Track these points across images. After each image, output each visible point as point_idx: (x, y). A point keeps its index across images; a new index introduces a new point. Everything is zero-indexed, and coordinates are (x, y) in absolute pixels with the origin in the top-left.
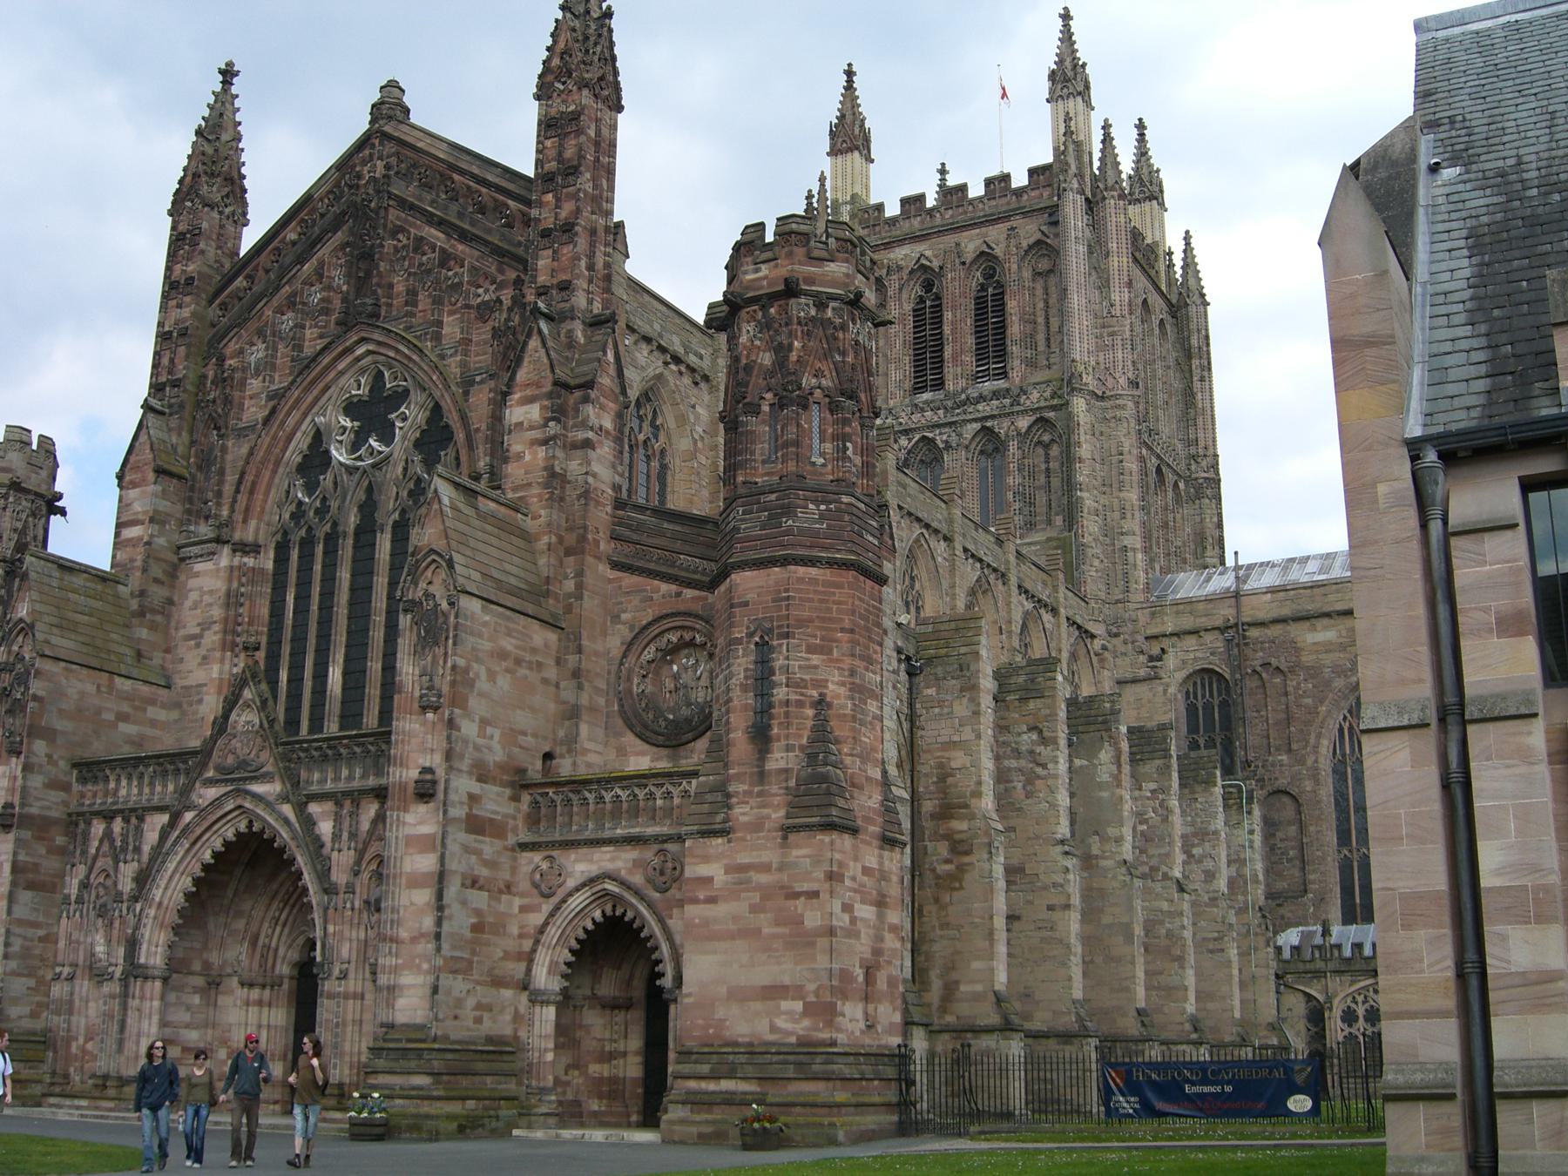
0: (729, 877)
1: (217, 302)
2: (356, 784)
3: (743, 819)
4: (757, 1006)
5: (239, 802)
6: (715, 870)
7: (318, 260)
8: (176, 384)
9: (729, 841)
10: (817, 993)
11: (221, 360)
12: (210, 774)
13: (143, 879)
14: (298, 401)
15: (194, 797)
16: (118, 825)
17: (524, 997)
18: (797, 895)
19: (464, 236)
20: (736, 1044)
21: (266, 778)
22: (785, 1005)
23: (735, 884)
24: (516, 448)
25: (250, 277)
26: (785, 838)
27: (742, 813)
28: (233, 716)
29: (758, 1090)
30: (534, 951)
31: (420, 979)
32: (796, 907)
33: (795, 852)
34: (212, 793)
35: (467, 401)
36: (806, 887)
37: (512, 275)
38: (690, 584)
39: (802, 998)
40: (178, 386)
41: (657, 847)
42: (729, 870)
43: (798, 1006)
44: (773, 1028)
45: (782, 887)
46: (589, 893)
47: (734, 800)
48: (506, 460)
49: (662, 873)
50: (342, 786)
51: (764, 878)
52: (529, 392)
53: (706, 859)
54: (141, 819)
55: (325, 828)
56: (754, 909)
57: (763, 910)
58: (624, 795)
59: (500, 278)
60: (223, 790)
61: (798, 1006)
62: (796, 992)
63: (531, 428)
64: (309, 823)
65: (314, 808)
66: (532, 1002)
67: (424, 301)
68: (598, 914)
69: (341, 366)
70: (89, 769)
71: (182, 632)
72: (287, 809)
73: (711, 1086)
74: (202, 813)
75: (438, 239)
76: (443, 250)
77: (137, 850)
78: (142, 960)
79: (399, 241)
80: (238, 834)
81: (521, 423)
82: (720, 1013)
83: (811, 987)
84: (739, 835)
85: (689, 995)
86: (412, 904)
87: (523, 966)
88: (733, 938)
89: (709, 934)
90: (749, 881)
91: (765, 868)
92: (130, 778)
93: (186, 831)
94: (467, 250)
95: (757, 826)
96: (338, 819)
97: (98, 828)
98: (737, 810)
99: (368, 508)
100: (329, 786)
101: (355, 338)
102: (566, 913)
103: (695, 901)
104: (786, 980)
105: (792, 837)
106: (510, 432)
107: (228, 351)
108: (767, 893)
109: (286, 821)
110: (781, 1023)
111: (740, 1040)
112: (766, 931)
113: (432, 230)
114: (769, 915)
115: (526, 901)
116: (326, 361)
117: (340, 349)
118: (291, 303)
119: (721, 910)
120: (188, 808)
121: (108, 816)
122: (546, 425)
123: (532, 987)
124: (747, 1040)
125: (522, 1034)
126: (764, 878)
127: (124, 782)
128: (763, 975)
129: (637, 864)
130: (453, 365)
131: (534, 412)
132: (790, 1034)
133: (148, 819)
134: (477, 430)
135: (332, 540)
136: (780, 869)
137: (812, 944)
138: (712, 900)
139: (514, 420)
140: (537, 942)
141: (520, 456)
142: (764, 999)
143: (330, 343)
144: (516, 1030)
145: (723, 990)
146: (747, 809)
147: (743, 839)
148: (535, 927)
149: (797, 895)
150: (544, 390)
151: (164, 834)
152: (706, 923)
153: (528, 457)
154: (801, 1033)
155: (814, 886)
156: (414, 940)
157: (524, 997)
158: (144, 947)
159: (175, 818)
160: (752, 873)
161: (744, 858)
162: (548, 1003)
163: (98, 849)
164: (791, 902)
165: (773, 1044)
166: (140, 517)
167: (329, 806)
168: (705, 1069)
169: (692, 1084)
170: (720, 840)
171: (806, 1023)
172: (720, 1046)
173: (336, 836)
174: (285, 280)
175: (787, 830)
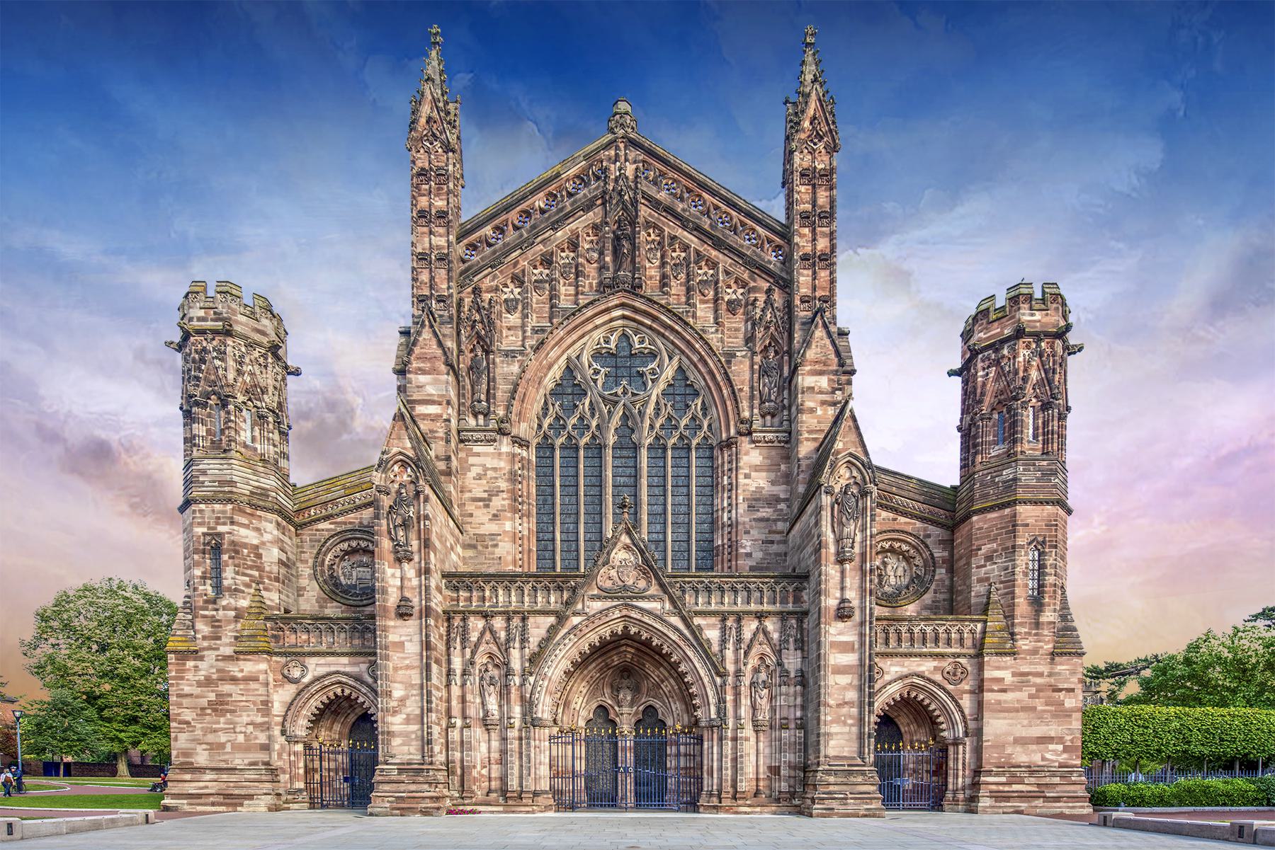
0: (1015, 679)
1: (466, 241)
2: (740, 607)
3: (1024, 647)
5: (625, 612)
6: (1007, 676)
7: (572, 231)
8: (441, 300)
9: (1015, 659)
10: (1072, 741)
11: (477, 291)
12: (596, 592)
13: (535, 660)
14: (562, 339)
15: (580, 606)
16: (498, 623)
18: (1060, 690)
19: (719, 244)
21: (651, 598)
24: (809, 404)
25: (500, 230)
27: (1024, 644)
28: (613, 555)
33: (1059, 667)
34: (598, 605)
35: (730, 368)
36: (1066, 686)
37: (765, 285)
38: (904, 514)
40: (444, 301)
42: (1014, 674)
47: (1018, 637)
48: (799, 411)
50: (726, 608)
51: (1038, 680)
52: (818, 367)
53: (998, 668)
54: (524, 619)
55: (712, 634)
56: (1031, 696)
57: (1038, 698)
58: (929, 630)
59: (752, 284)
60: (609, 604)
61: (1060, 747)
62: (1060, 740)
63: (821, 392)
64: (696, 632)
65: (697, 621)
67: (676, 288)
69: (598, 321)
70: (455, 580)
71: (467, 495)
72: (675, 621)
74: (590, 618)
75: (691, 241)
76: (698, 253)
77: (524, 641)
78: (539, 715)
79: (649, 235)
80: (613, 634)
81: (813, 388)
83: (1069, 738)
88: (1017, 711)
89: (1002, 709)
90: (1028, 681)
91: (1041, 675)
92: (507, 589)
93: (575, 627)
94: (721, 256)
95: (1034, 652)
96: (724, 630)
97: (477, 624)
98: (1020, 643)
99: (629, 425)
100: (713, 607)
101: (616, 302)
103: (993, 691)
105: (1057, 659)
106: (803, 393)
107: (483, 287)
108: (1040, 689)
109: (676, 629)
112: (1039, 708)
113: (685, 233)
116: (590, 314)
117: (603, 307)
118: (547, 261)
119: (1009, 696)
120: (576, 614)
121: (486, 616)
122: (833, 392)
126: (1038, 680)
127: (501, 592)
128: (1038, 731)
130: (715, 340)
131: (823, 382)
133: (531, 621)
134: (741, 390)
135: (597, 449)
136: (1050, 675)
137: (1070, 716)
138: (1004, 691)
139: (806, 385)
141: (812, 411)
143: (595, 300)
146: (1027, 642)
149: (1060, 690)
150: (831, 368)
151: (553, 630)
152: (999, 702)
153: (819, 412)
155: (1072, 686)
158: (540, 706)
159: (561, 618)
160: (1030, 677)
161: (1025, 669)
163: (480, 639)
166: (436, 398)
167: (713, 620)
171: (1065, 756)
173: (723, 641)
174: (539, 239)
175: (1053, 655)
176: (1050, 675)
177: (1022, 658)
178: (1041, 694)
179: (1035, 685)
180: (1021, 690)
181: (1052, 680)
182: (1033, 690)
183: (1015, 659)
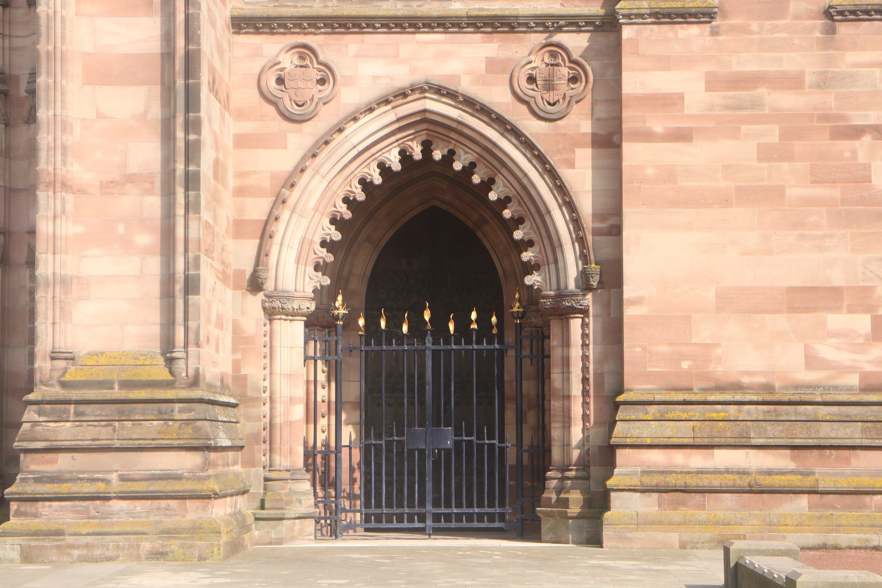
0: (717, 97)
4: (780, 322)
9: (714, 33)
17: (255, 303)
18: (857, 132)
20: (738, 387)
22: (836, 321)
23: (727, 107)
26: (831, 31)
29: (792, 466)
30: (272, 218)
31: (131, 265)
32: (854, 153)
33: (851, 57)
39: (868, 309)
41: (539, 38)
42: (713, 83)
43: (863, 323)
44: (812, 361)
45: (825, 118)
46: (392, 117)
49: (549, 86)
51: (787, 101)
53: (665, 62)
56: (766, 154)
57: (788, 157)
66: (271, 314)
68: (394, 161)
73: (697, 460)
82: (703, 333)
84: (734, 21)
85: (638, 301)
86: (100, 116)
87: (250, 247)
88: (726, 202)
102: (341, 151)
103: (647, 136)
104: (837, 279)
105: (844, 29)
110: (826, 351)
111: (746, 380)
112: (793, 192)
114: (799, 165)
115: (249, 127)
123: (269, 286)
124: (760, 380)
125: (254, 371)
126: (787, 101)
129: (493, 66)
132: (850, 370)
136: (824, 82)
138: (682, 136)
140: (280, 201)
142: (792, 310)
144: (236, 365)
145: (710, 295)
147: (745, 30)
148: (273, 176)
149: (857, 132)
152: (669, 175)
154: (869, 368)
156: (109, 187)
157: (255, 303)
162: (294, 314)
164: (844, 146)
165: (813, 387)
168: (682, 432)
169: (656, 457)
170: (694, 30)
172: (705, 390)
176: (824, 82)
177: (734, 29)
178: (799, 146)
179: (776, 116)
180: (734, 134)
181: (829, 100)
182: (772, 134)
183: (714, 33)
